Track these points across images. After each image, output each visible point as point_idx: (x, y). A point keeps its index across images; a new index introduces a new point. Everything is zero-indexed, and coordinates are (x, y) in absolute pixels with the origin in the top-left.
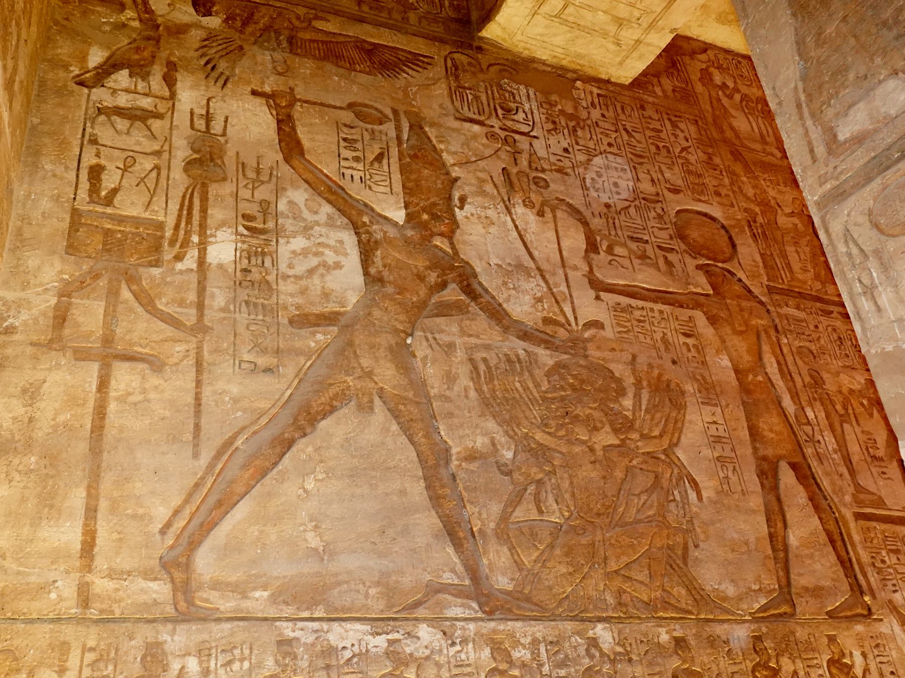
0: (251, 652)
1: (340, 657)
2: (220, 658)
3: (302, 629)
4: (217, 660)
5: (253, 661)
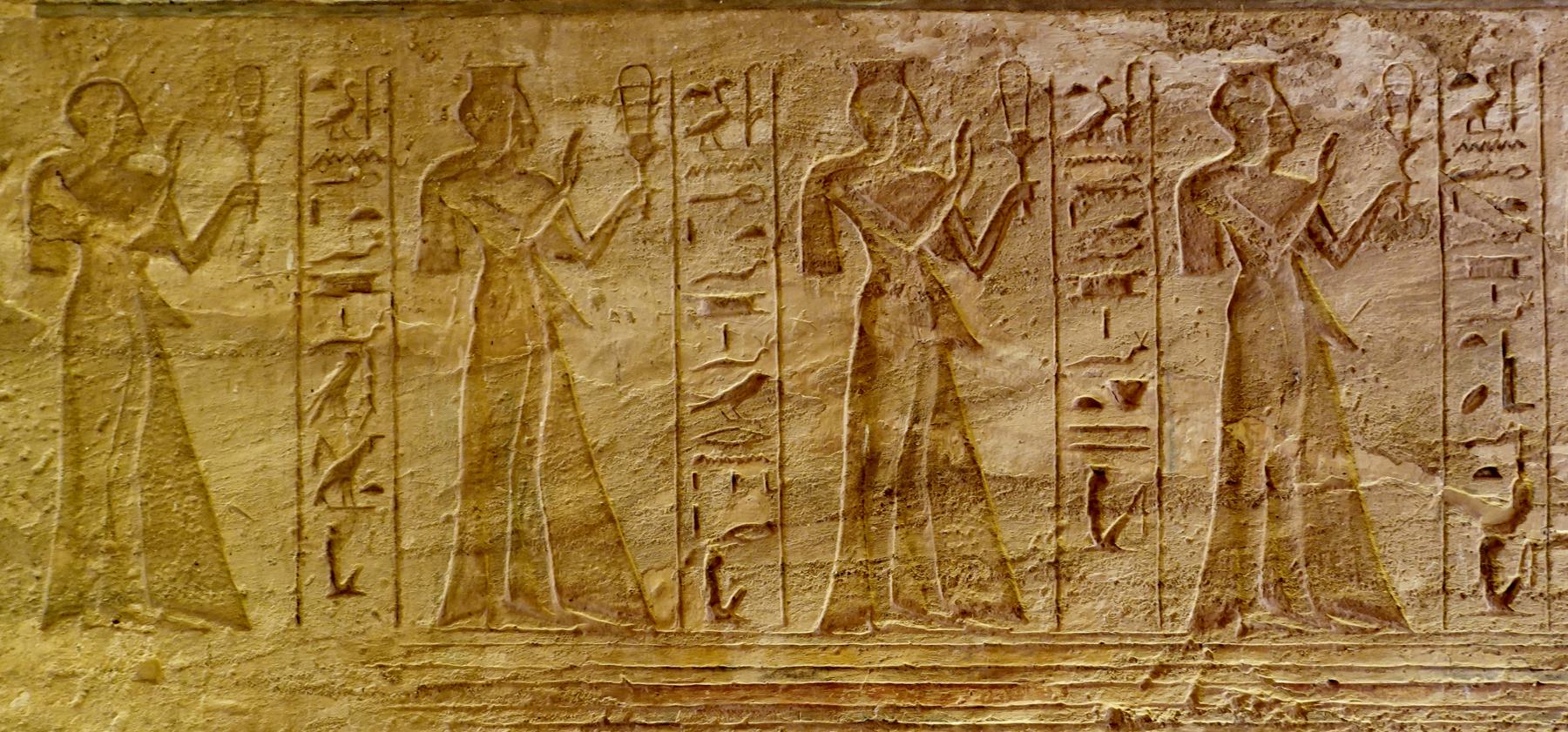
0: (775, 97)
1: (1058, 114)
2: (681, 111)
3: (939, 33)
4: (673, 117)
5: (781, 121)
